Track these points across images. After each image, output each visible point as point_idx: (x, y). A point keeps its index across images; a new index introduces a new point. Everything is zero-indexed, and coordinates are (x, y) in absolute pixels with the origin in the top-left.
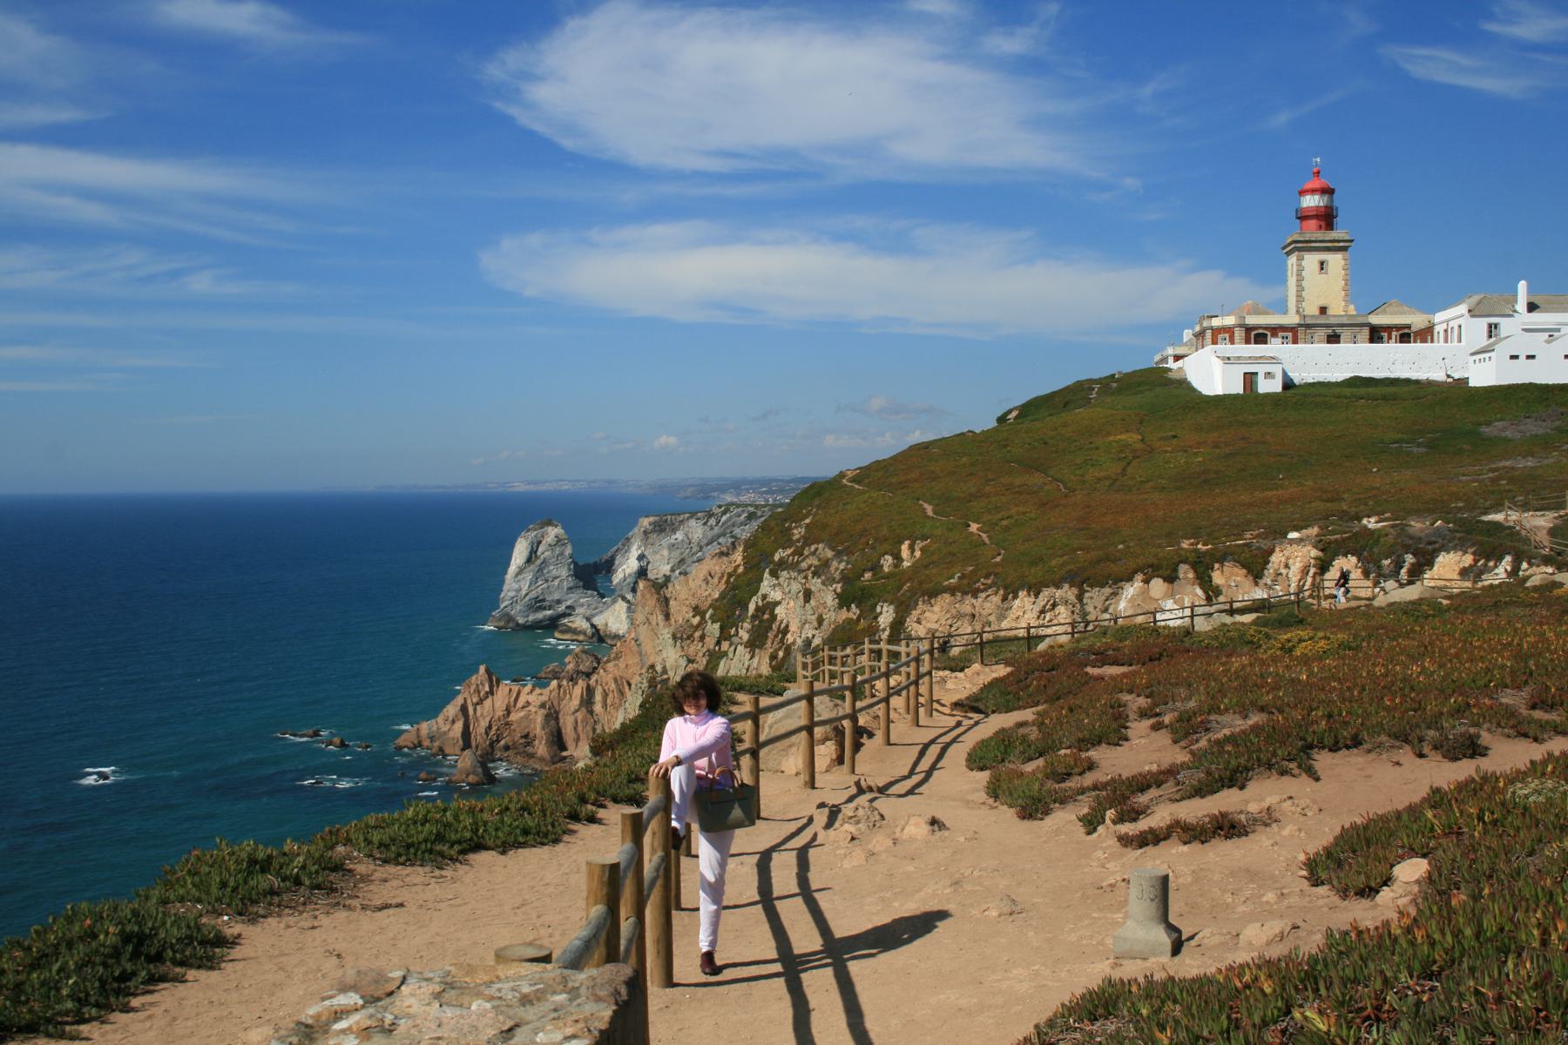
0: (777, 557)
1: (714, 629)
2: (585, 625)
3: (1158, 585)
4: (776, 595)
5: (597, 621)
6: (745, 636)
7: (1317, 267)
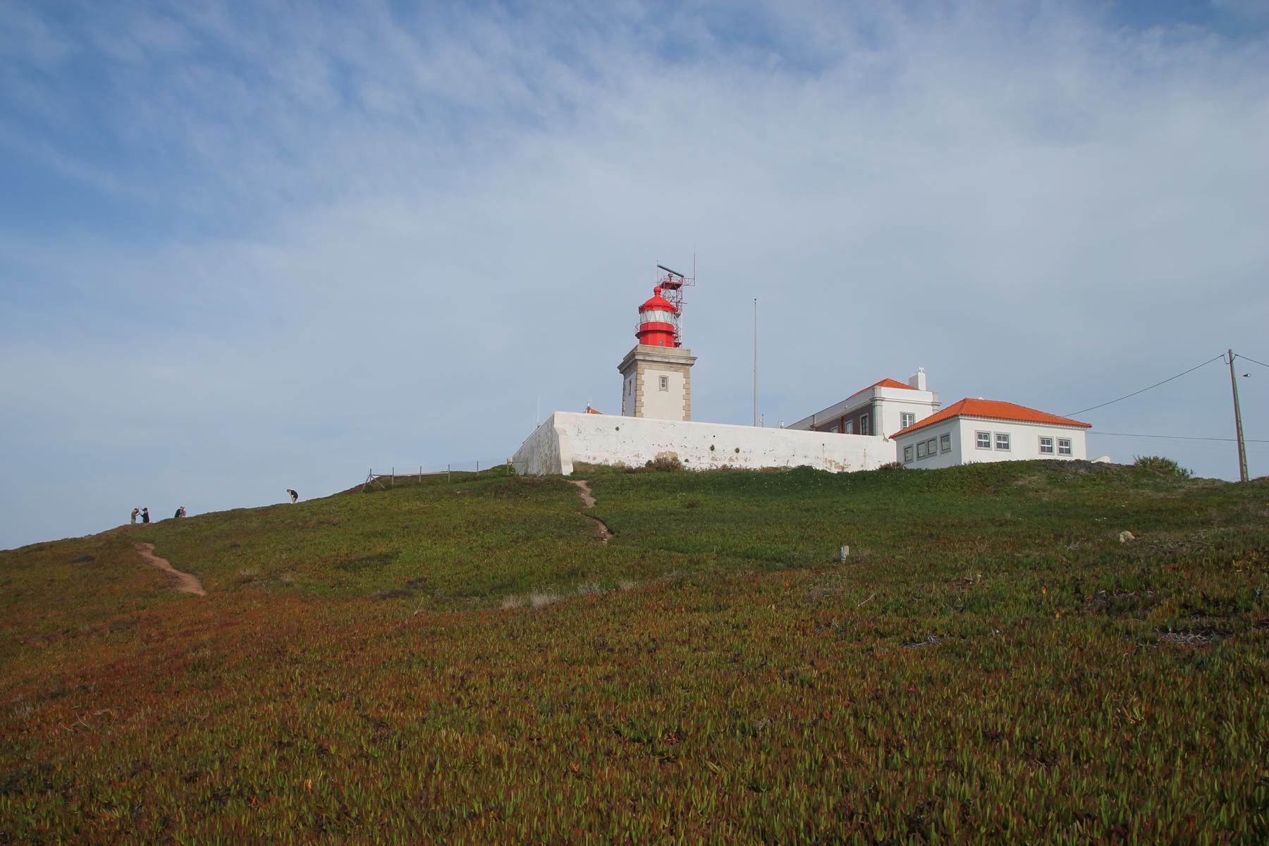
7: (657, 383)
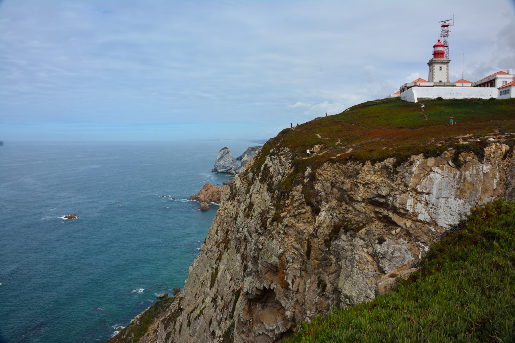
0: (271, 151)
1: (251, 174)
2: (234, 172)
3: (431, 161)
4: (270, 164)
5: (237, 171)
6: (260, 177)
7: (439, 68)
